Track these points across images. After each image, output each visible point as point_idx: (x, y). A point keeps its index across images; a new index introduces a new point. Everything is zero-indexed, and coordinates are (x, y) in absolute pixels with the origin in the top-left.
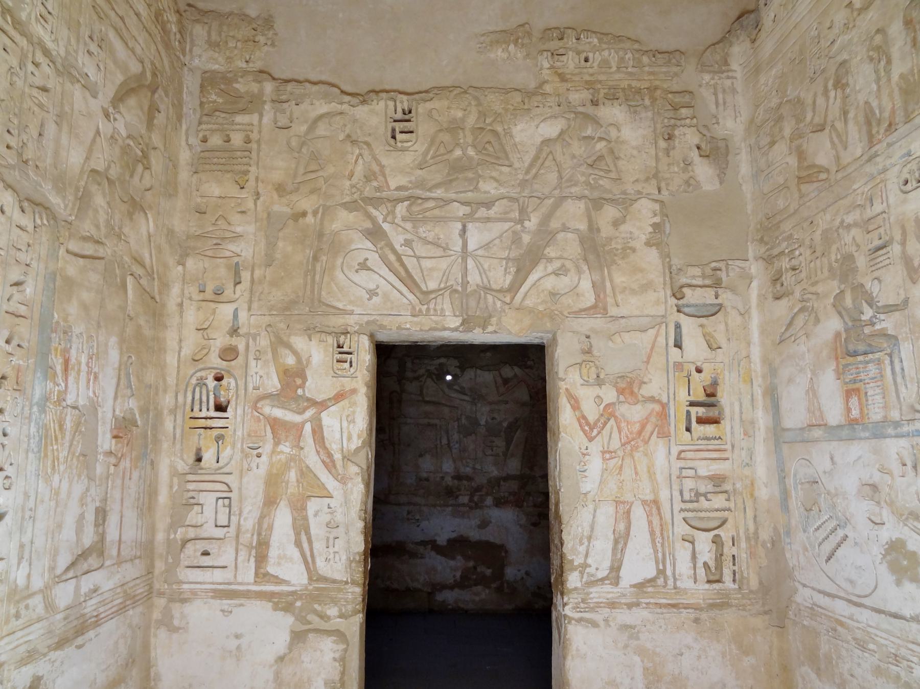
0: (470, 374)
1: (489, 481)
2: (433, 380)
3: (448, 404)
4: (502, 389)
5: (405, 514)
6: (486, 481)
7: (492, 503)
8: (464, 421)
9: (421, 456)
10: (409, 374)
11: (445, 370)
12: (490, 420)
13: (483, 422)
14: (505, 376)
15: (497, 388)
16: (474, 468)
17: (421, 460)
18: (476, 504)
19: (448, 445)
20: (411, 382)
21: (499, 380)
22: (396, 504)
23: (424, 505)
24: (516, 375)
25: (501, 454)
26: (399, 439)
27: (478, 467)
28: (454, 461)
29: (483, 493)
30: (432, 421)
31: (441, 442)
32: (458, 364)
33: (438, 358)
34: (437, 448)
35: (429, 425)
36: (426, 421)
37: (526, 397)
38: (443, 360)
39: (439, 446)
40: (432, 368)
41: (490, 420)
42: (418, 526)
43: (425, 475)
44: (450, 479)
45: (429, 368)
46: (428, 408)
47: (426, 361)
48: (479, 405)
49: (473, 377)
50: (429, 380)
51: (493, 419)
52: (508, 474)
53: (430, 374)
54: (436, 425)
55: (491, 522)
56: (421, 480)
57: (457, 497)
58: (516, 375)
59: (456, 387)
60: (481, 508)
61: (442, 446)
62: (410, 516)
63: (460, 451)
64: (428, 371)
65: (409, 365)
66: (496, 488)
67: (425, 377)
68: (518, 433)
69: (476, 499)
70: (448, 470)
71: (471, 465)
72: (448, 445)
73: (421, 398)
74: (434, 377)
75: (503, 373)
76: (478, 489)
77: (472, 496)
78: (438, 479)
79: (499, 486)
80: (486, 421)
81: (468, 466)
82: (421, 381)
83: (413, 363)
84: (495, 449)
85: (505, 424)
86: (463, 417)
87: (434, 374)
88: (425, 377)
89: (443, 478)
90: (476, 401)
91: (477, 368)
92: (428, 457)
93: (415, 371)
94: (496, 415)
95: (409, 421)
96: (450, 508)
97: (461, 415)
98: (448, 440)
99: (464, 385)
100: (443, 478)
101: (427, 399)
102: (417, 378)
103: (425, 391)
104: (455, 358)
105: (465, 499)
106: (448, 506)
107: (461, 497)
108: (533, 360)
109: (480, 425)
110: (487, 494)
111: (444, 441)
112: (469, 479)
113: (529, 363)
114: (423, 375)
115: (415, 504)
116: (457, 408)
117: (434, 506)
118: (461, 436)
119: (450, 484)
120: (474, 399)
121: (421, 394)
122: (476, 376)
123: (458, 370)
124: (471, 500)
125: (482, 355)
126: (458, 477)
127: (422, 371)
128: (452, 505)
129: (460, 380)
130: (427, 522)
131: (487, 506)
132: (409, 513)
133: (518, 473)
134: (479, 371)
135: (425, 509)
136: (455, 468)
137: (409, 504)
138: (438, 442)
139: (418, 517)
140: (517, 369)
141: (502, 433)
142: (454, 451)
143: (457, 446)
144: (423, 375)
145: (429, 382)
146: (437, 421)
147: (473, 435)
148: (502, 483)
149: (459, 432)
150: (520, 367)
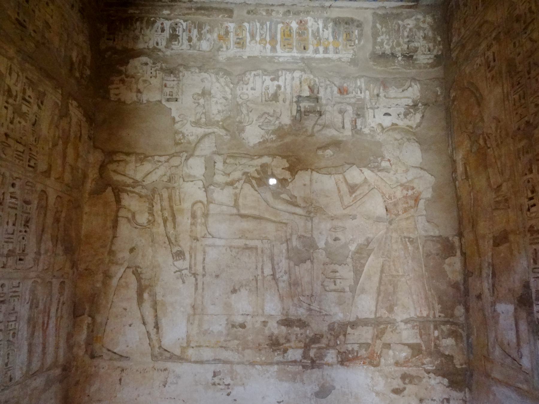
0: (303, 177)
1: (331, 328)
2: (253, 186)
3: (273, 218)
4: (348, 200)
5: (210, 375)
6: (325, 328)
7: (335, 360)
8: (295, 243)
9: (234, 291)
10: (220, 178)
11: (269, 173)
12: (330, 241)
13: (321, 244)
14: (350, 182)
15: (341, 198)
16: (310, 310)
17: (233, 296)
18: (313, 361)
19: (273, 275)
20: (222, 189)
21: (344, 188)
22: (196, 362)
23: (238, 363)
24: (366, 181)
25: (347, 289)
26: (204, 268)
27: (315, 306)
28: (281, 298)
29: (323, 345)
30: (251, 243)
31: (263, 272)
32: (287, 165)
33: (260, 156)
34: (257, 281)
35: (247, 248)
36: (241, 243)
37: (381, 211)
38: (266, 160)
39: (260, 277)
40: (252, 170)
41: (330, 241)
42: (228, 395)
43: (239, 319)
44: (276, 325)
45: (246, 170)
46: (246, 225)
47: (244, 161)
48: (316, 220)
49: (308, 183)
50: (247, 187)
51: (336, 239)
52: (357, 318)
53: (248, 178)
54: (256, 248)
55: (334, 388)
56: (233, 326)
57: (285, 351)
58: (366, 181)
59: (284, 196)
60: (320, 366)
61: (264, 277)
62: (216, 380)
63: (290, 284)
64: (245, 173)
65: (219, 165)
66: (341, 337)
67: (242, 182)
68: (370, 259)
69: (312, 353)
70: (273, 313)
71: (305, 305)
72: (273, 275)
73: (235, 211)
74: (254, 182)
75: (348, 177)
76: (316, 339)
77: (307, 347)
78: (258, 325)
79: (345, 335)
80: (326, 243)
81: (300, 307)
82: (236, 188)
83: (225, 162)
84: (338, 281)
85: (353, 247)
86: (294, 238)
87: (254, 178)
88: (242, 182)
89: (265, 323)
90: (312, 215)
91: (312, 170)
92: (244, 292)
93: (229, 175)
94: (340, 235)
95: (218, 242)
96: (276, 367)
97: (291, 235)
98: (273, 268)
99: (296, 194)
100: (265, 323)
101: (243, 212)
102: (231, 184)
103: (241, 201)
104: (283, 157)
105: (295, 354)
106: (271, 364)
107: (290, 352)
108: (389, 160)
109: (317, 248)
110: (328, 347)
111: (268, 271)
112: (302, 324)
113: (384, 164)
114: (238, 180)
115: (225, 362)
116: (286, 224)
117: (252, 364)
118: (292, 264)
119: (276, 332)
120: (310, 212)
121: (236, 205)
122: (311, 181)
123: (287, 173)
124: (305, 356)
125: (320, 152)
126: (287, 322)
127: (237, 175)
128: (278, 363)
129: (290, 187)
130: (241, 388)
131: (328, 364)
132: (215, 375)
133: (373, 316)
134: (315, 175)
135: (238, 368)
136: (283, 309)
137: (217, 361)
138: (259, 272)
139: (228, 381)
140: (367, 173)
141: (349, 260)
142: (281, 285)
143: (285, 278)
144: (238, 180)
145: (247, 188)
146: (257, 243)
147: (308, 262)
148: (349, 330)
149: (288, 258)
150: (371, 169)
